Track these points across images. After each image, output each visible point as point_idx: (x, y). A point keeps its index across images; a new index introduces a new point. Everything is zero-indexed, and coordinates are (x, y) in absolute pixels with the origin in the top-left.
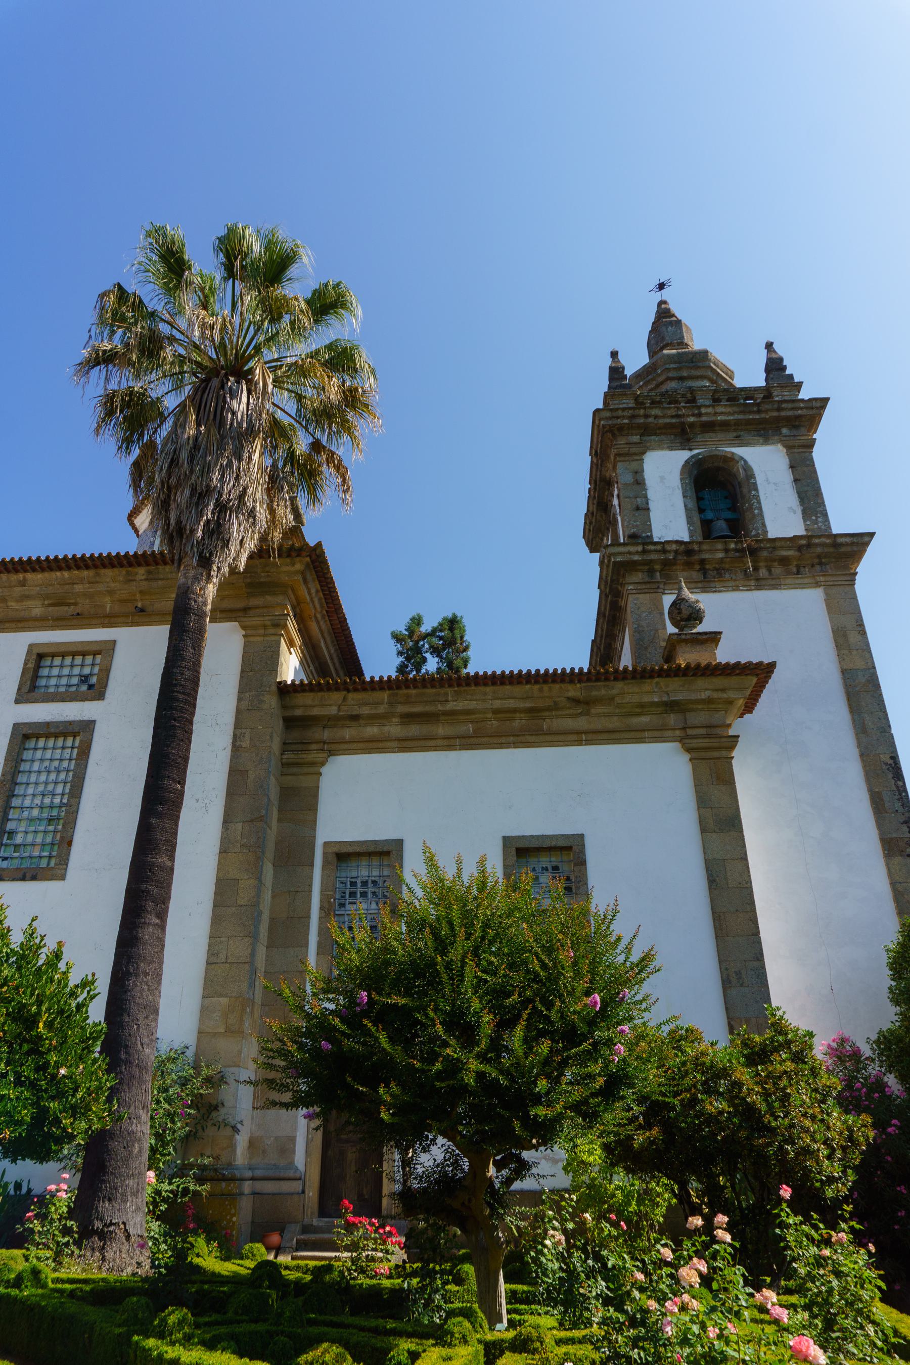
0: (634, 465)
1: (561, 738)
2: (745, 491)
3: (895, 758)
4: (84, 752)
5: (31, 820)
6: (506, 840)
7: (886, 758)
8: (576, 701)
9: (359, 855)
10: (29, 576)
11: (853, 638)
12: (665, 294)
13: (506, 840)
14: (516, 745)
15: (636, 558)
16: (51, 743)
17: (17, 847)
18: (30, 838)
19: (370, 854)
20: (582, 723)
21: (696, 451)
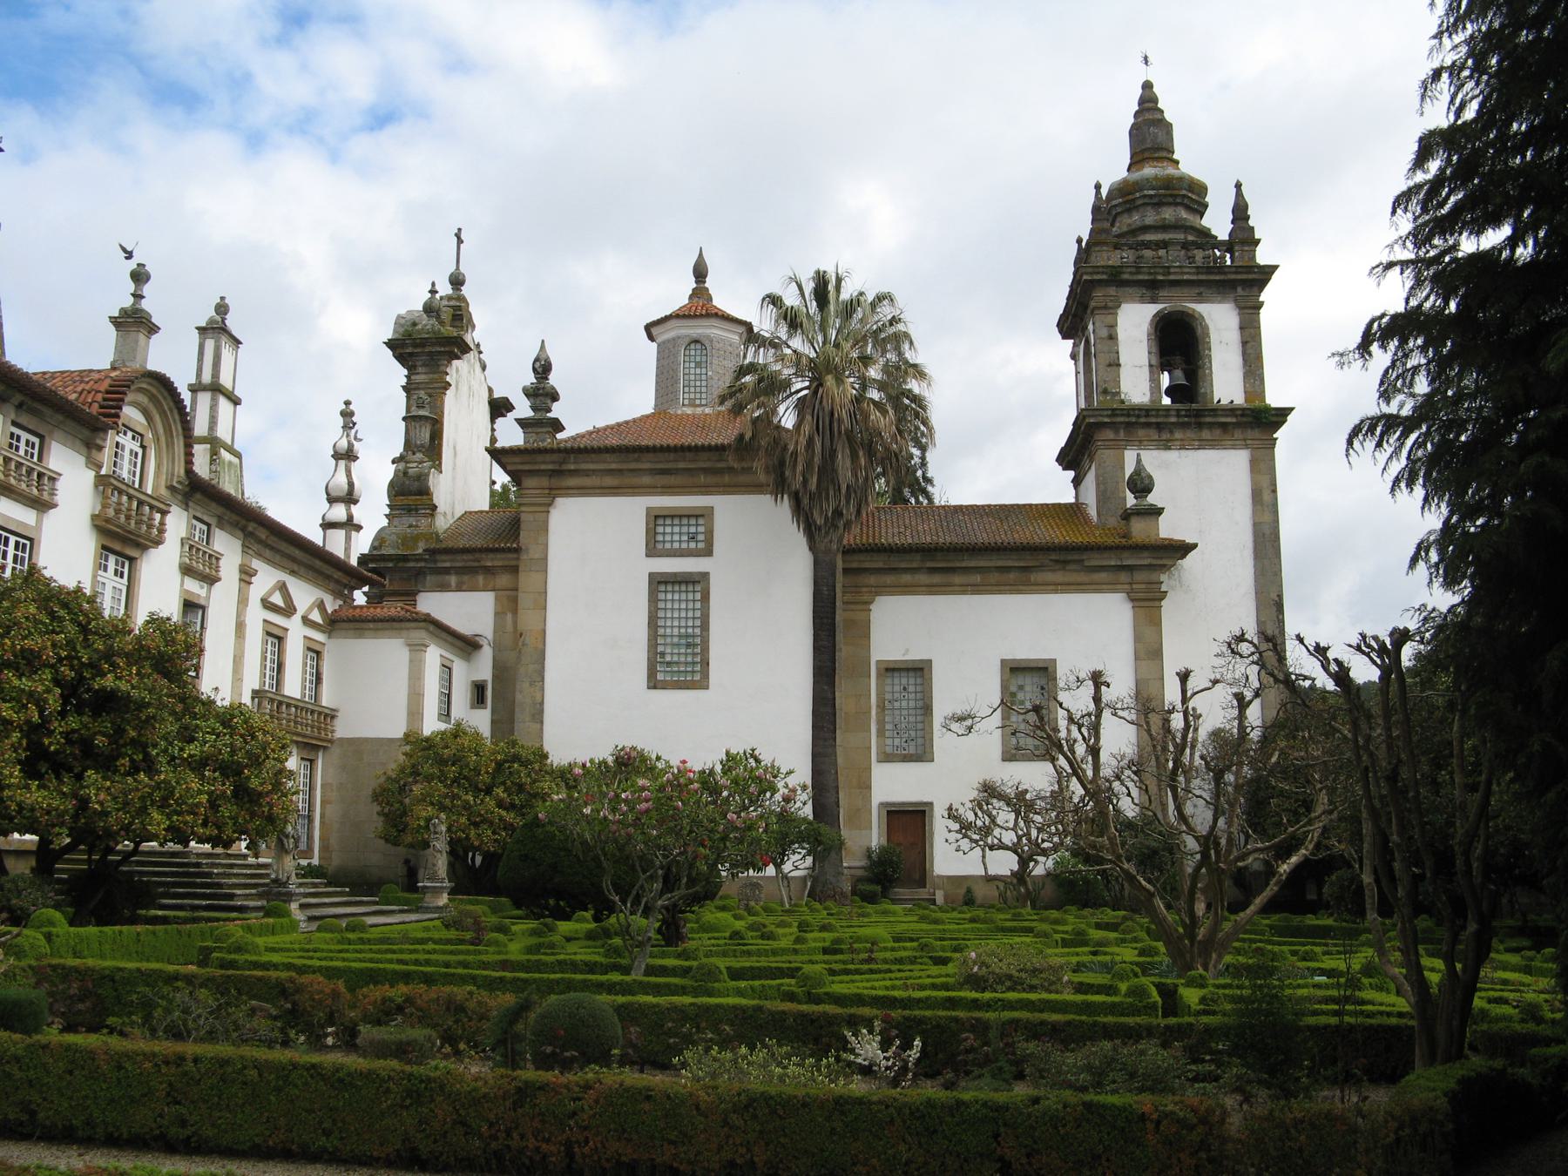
0: (1109, 319)
3: (1280, 597)
4: (706, 597)
5: (673, 645)
6: (1003, 662)
8: (1057, 561)
9: (899, 670)
11: (1266, 497)
13: (1003, 662)
14: (1011, 592)
15: (1106, 420)
16: (683, 588)
17: (669, 664)
18: (675, 658)
19: (908, 670)
21: (1161, 306)
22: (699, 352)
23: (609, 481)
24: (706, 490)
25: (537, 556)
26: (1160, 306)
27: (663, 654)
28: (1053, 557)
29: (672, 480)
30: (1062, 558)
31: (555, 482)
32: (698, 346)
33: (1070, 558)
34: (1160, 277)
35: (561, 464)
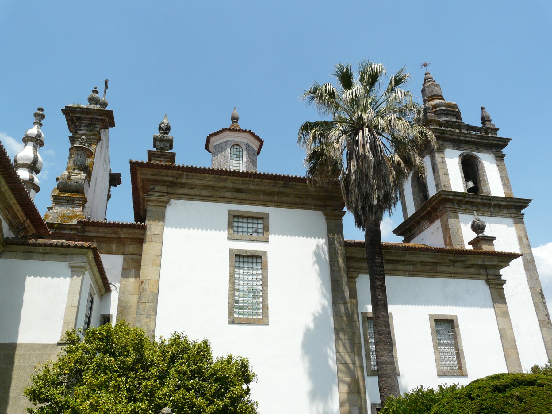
1: (445, 275)
2: (480, 172)
4: (264, 267)
7: (538, 290)
10: (229, 177)
12: (429, 69)
20: (451, 269)
22: (238, 150)
23: (205, 192)
24: (264, 203)
25: (156, 233)
26: (462, 152)
27: (237, 302)
28: (450, 258)
29: (243, 196)
30: (456, 259)
31: (171, 190)
32: (238, 147)
33: (459, 259)
34: (462, 138)
35: (177, 178)
